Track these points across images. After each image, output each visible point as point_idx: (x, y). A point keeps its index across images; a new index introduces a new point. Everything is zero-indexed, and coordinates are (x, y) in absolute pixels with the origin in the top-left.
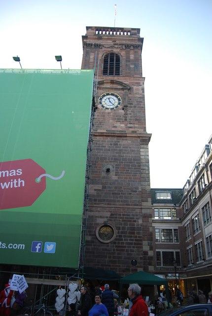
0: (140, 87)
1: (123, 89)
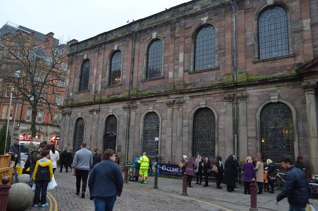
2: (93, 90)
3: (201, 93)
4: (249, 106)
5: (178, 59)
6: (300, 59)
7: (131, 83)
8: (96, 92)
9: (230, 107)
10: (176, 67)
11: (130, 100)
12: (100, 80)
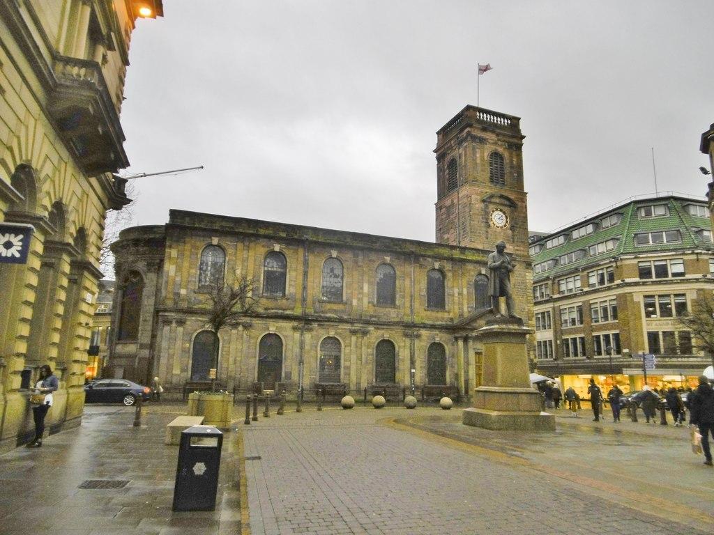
0: (524, 204)
1: (510, 206)
3: (385, 327)
5: (362, 288)
6: (451, 315)
7: (304, 300)
9: (408, 341)
10: (360, 296)
11: (305, 321)
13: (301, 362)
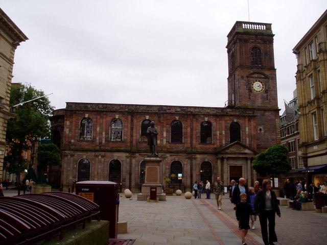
2: (98, 141)
4: (197, 162)
5: (163, 135)
6: (215, 146)
7: (131, 142)
8: (100, 143)
12: (104, 136)
13: (130, 174)
